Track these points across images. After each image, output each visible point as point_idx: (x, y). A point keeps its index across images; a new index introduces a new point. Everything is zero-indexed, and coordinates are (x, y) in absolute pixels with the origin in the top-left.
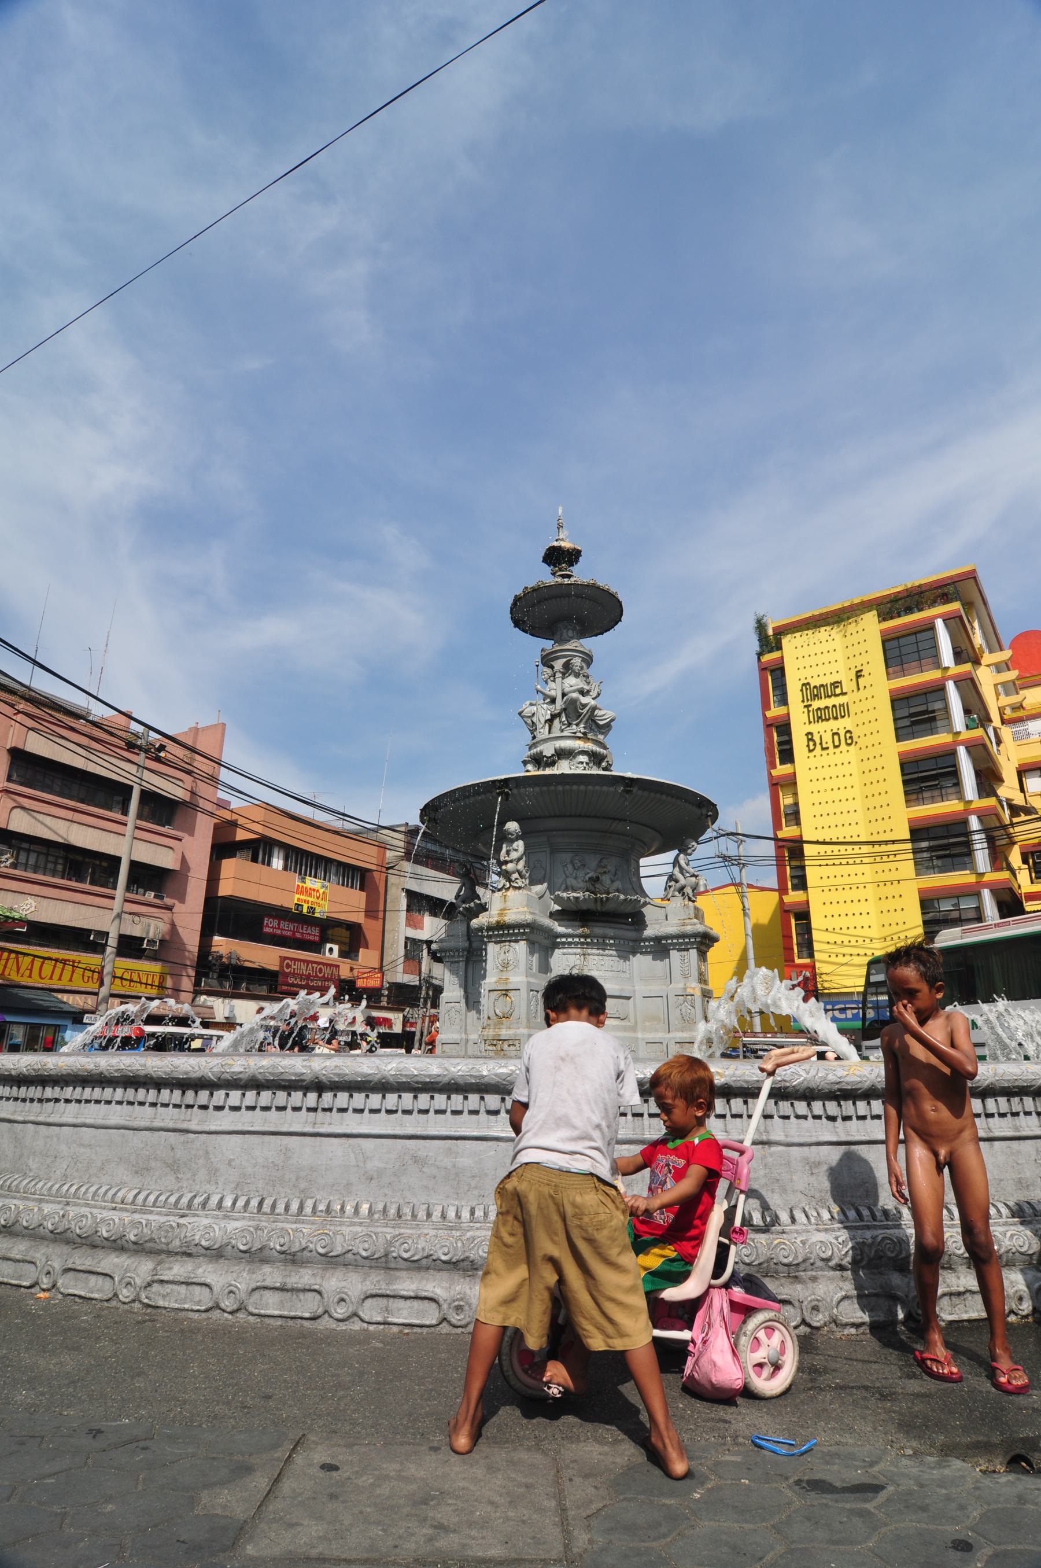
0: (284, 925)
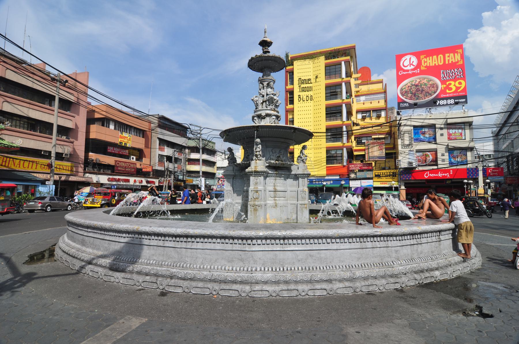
0: (115, 149)
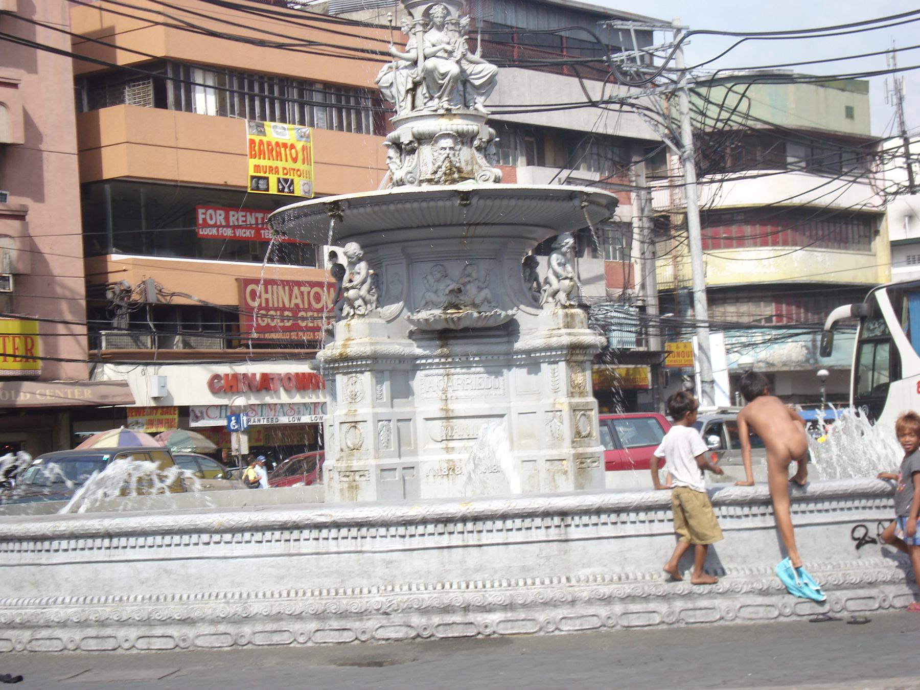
0: (236, 217)
